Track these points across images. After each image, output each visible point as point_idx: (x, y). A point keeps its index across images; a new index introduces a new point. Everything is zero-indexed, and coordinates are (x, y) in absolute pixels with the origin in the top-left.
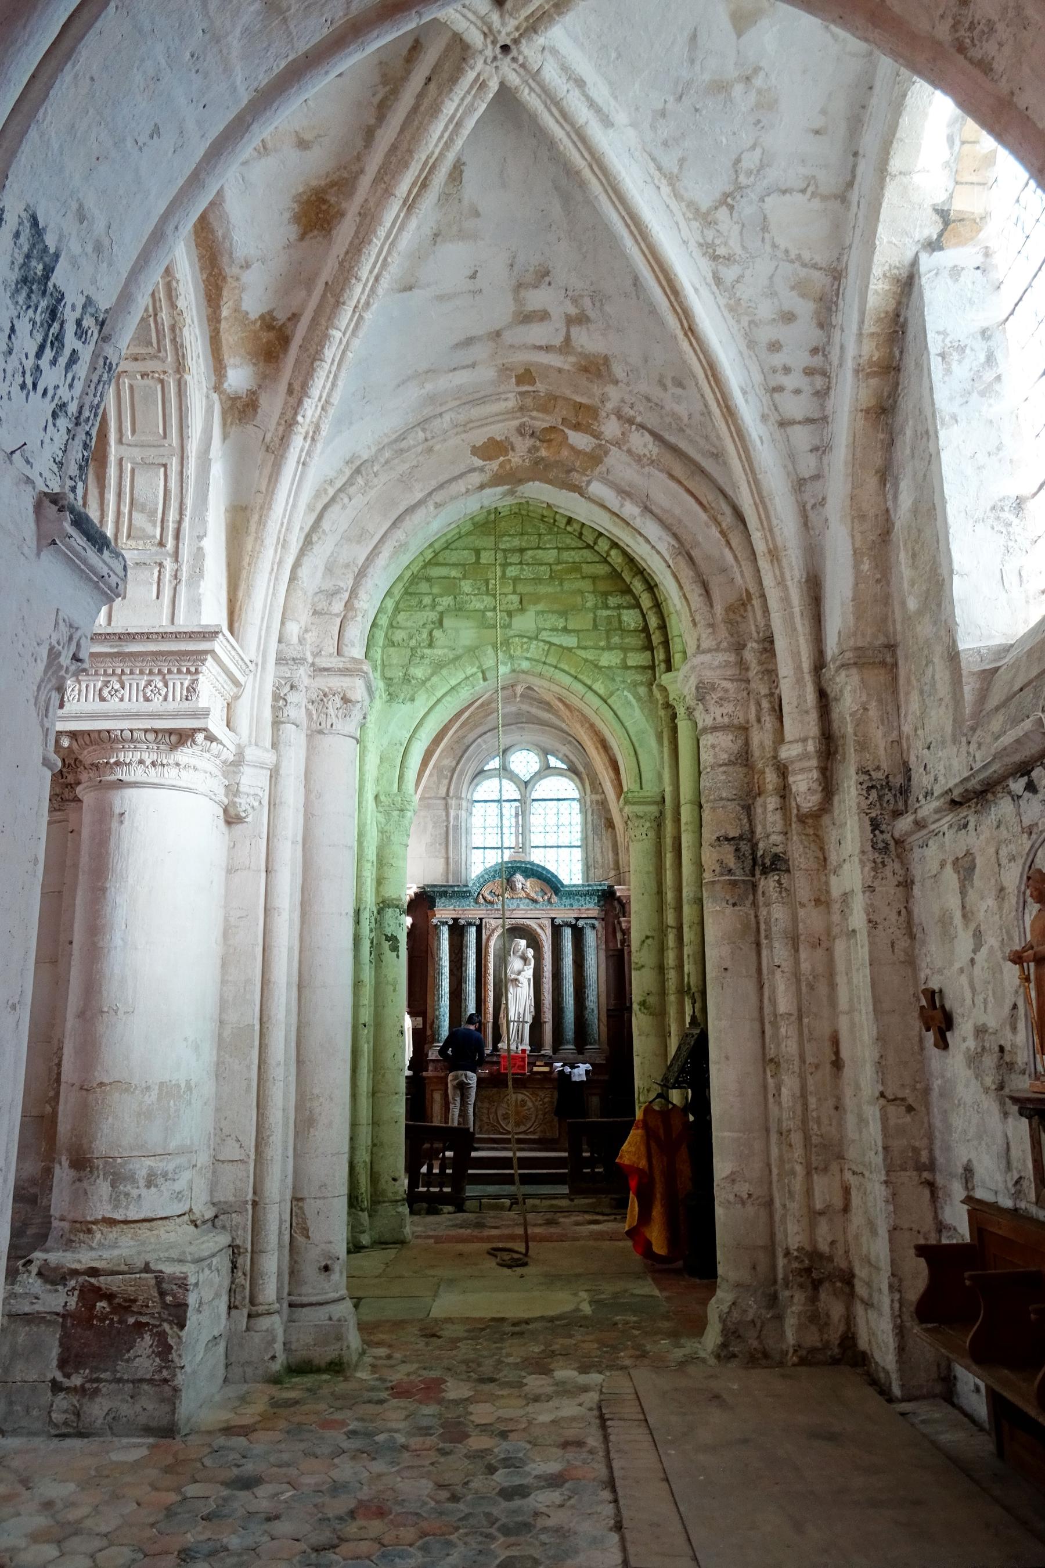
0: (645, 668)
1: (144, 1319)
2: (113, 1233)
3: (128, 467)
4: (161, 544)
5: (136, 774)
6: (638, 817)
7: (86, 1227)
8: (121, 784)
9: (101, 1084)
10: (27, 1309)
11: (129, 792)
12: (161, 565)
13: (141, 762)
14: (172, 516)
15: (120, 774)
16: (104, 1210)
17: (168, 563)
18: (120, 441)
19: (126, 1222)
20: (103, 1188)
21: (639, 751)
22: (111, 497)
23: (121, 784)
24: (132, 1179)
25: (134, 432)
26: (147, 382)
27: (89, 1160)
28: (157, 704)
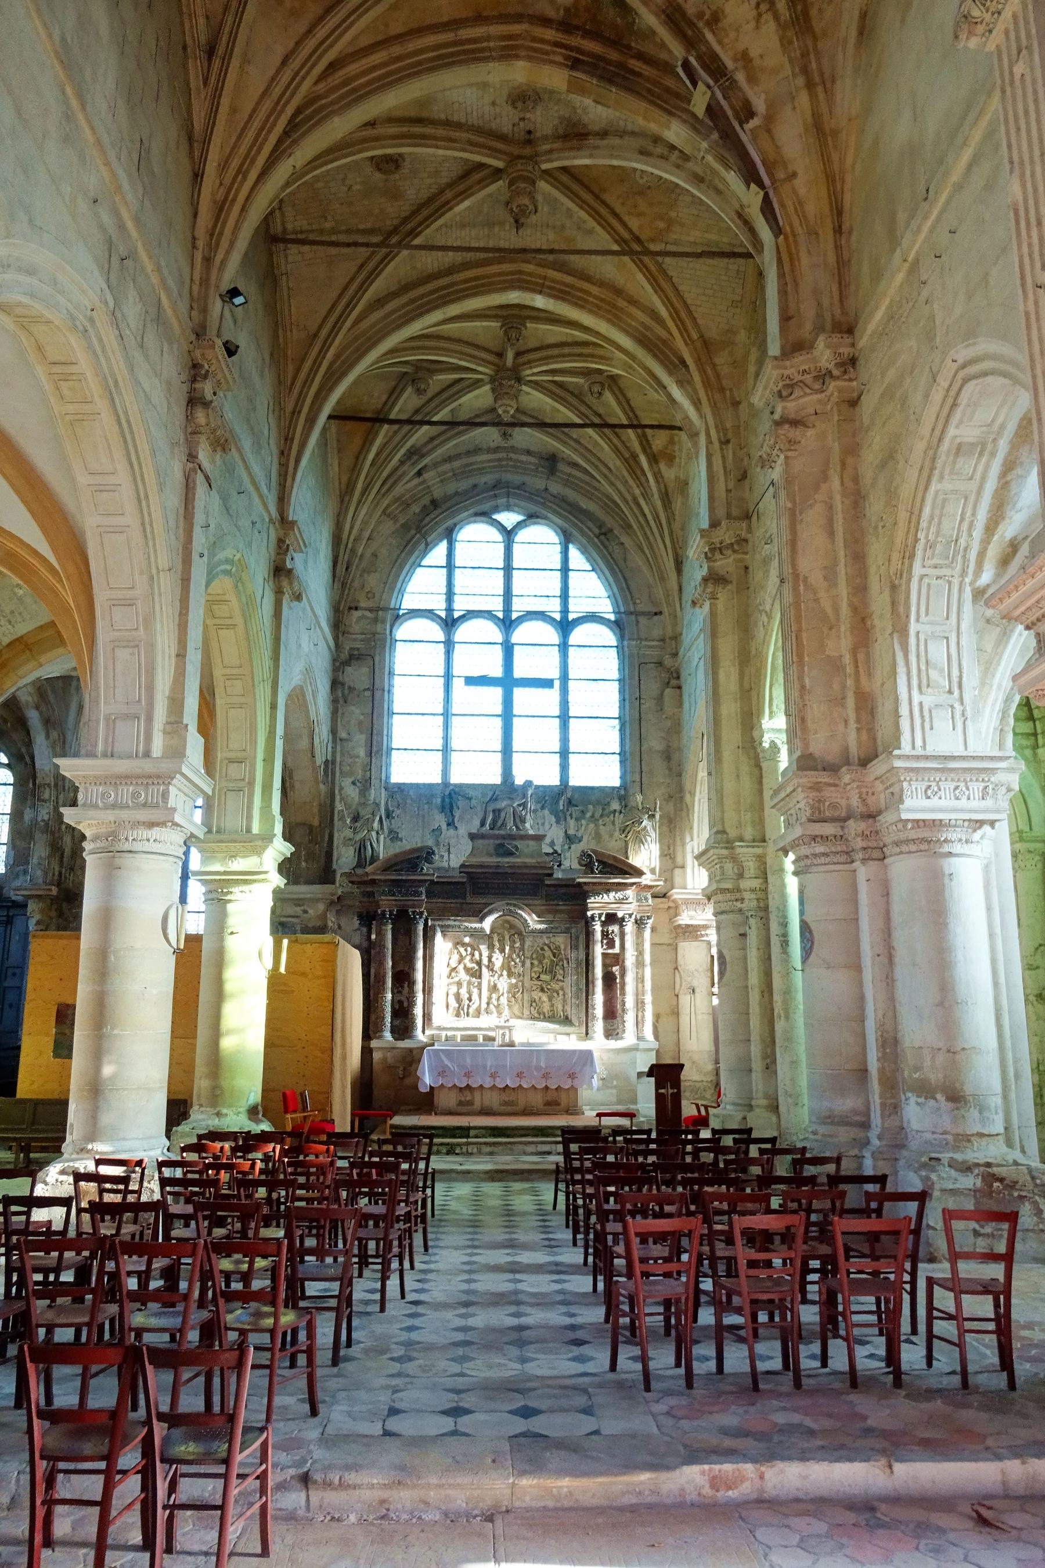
0: (1028, 735)
1: (1024, 1194)
2: (984, 1141)
3: (922, 638)
4: (950, 692)
5: (957, 848)
6: (1030, 852)
7: (967, 1138)
8: (950, 854)
9: (964, 1049)
10: (951, 1187)
11: (953, 860)
12: (952, 706)
13: (960, 840)
14: (955, 673)
15: (946, 848)
16: (977, 1128)
17: (957, 705)
18: (918, 620)
19: (989, 1135)
20: (974, 1113)
21: (1029, 800)
22: (913, 658)
23: (950, 854)
24: (988, 1108)
25: (927, 614)
26: (939, 581)
27: (964, 1097)
28: (963, 803)
